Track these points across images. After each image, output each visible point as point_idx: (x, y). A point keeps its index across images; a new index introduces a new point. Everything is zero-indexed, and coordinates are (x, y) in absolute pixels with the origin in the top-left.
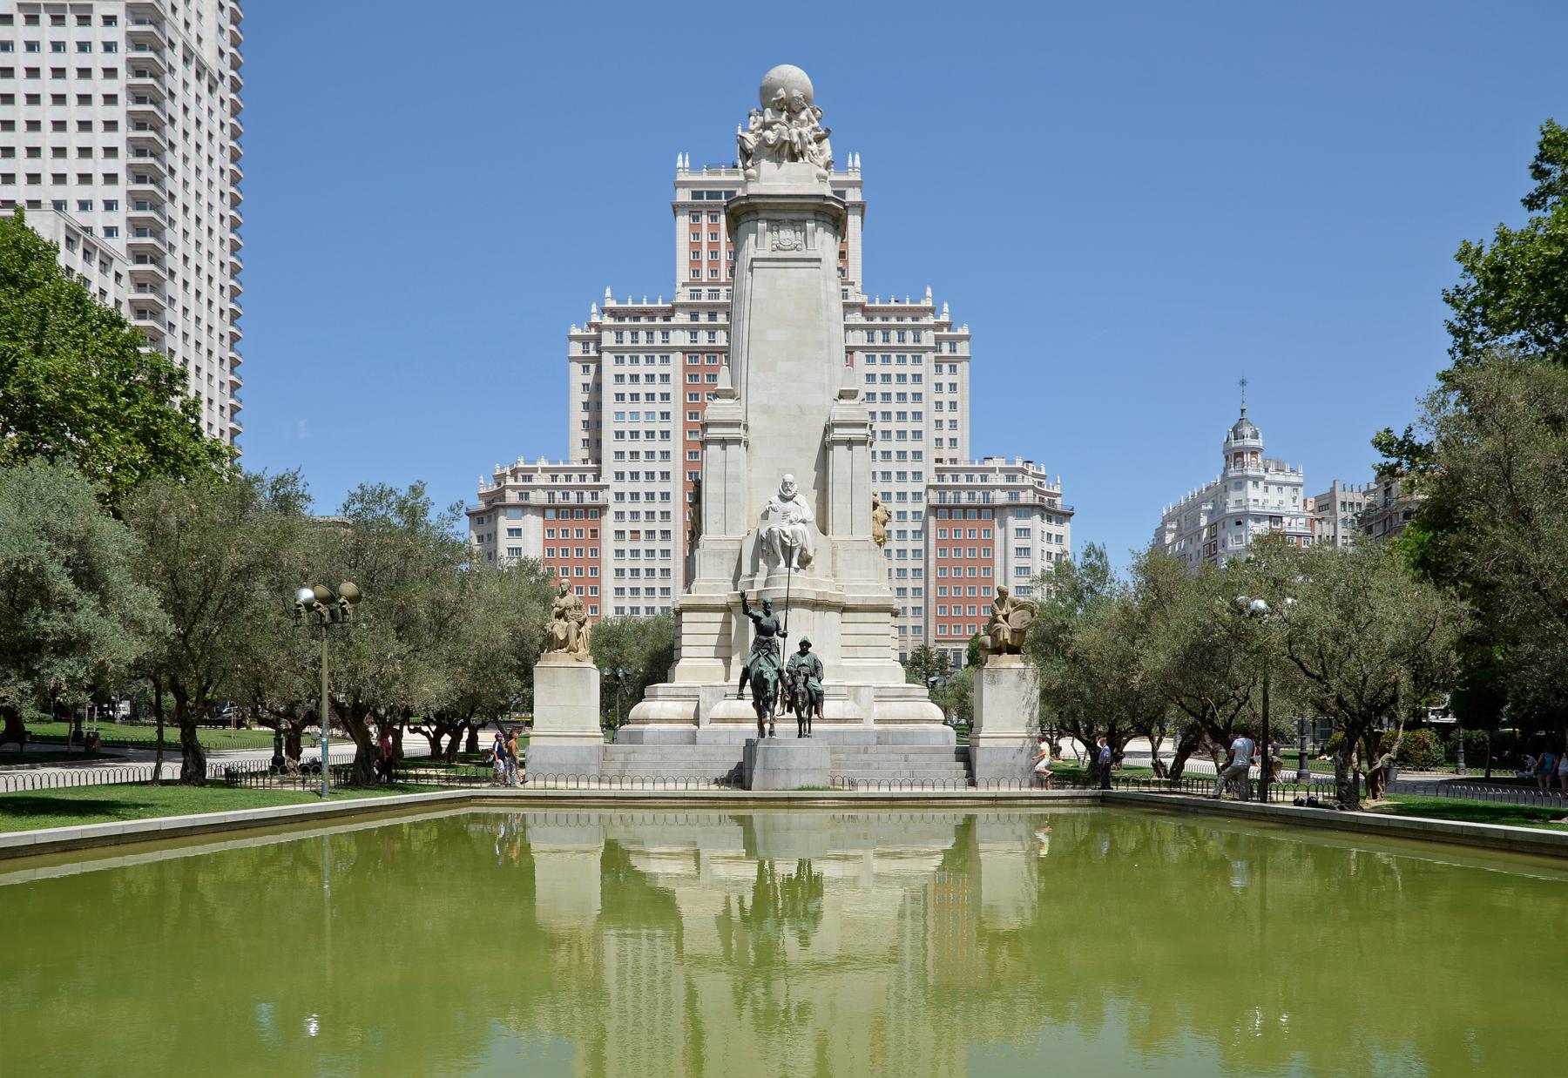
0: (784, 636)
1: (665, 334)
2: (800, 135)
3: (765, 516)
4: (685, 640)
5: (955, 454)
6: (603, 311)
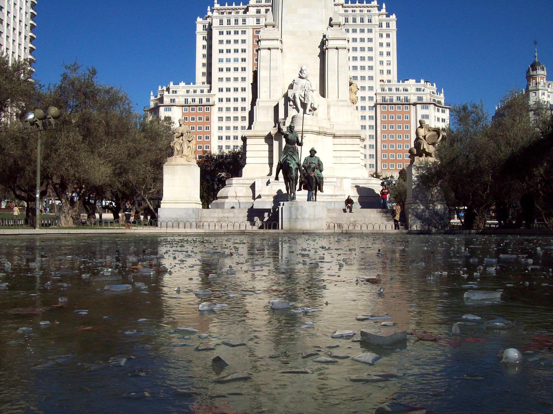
0: (301, 144)
1: (244, 21)
3: (291, 87)
4: (248, 154)
5: (390, 77)
6: (212, 11)
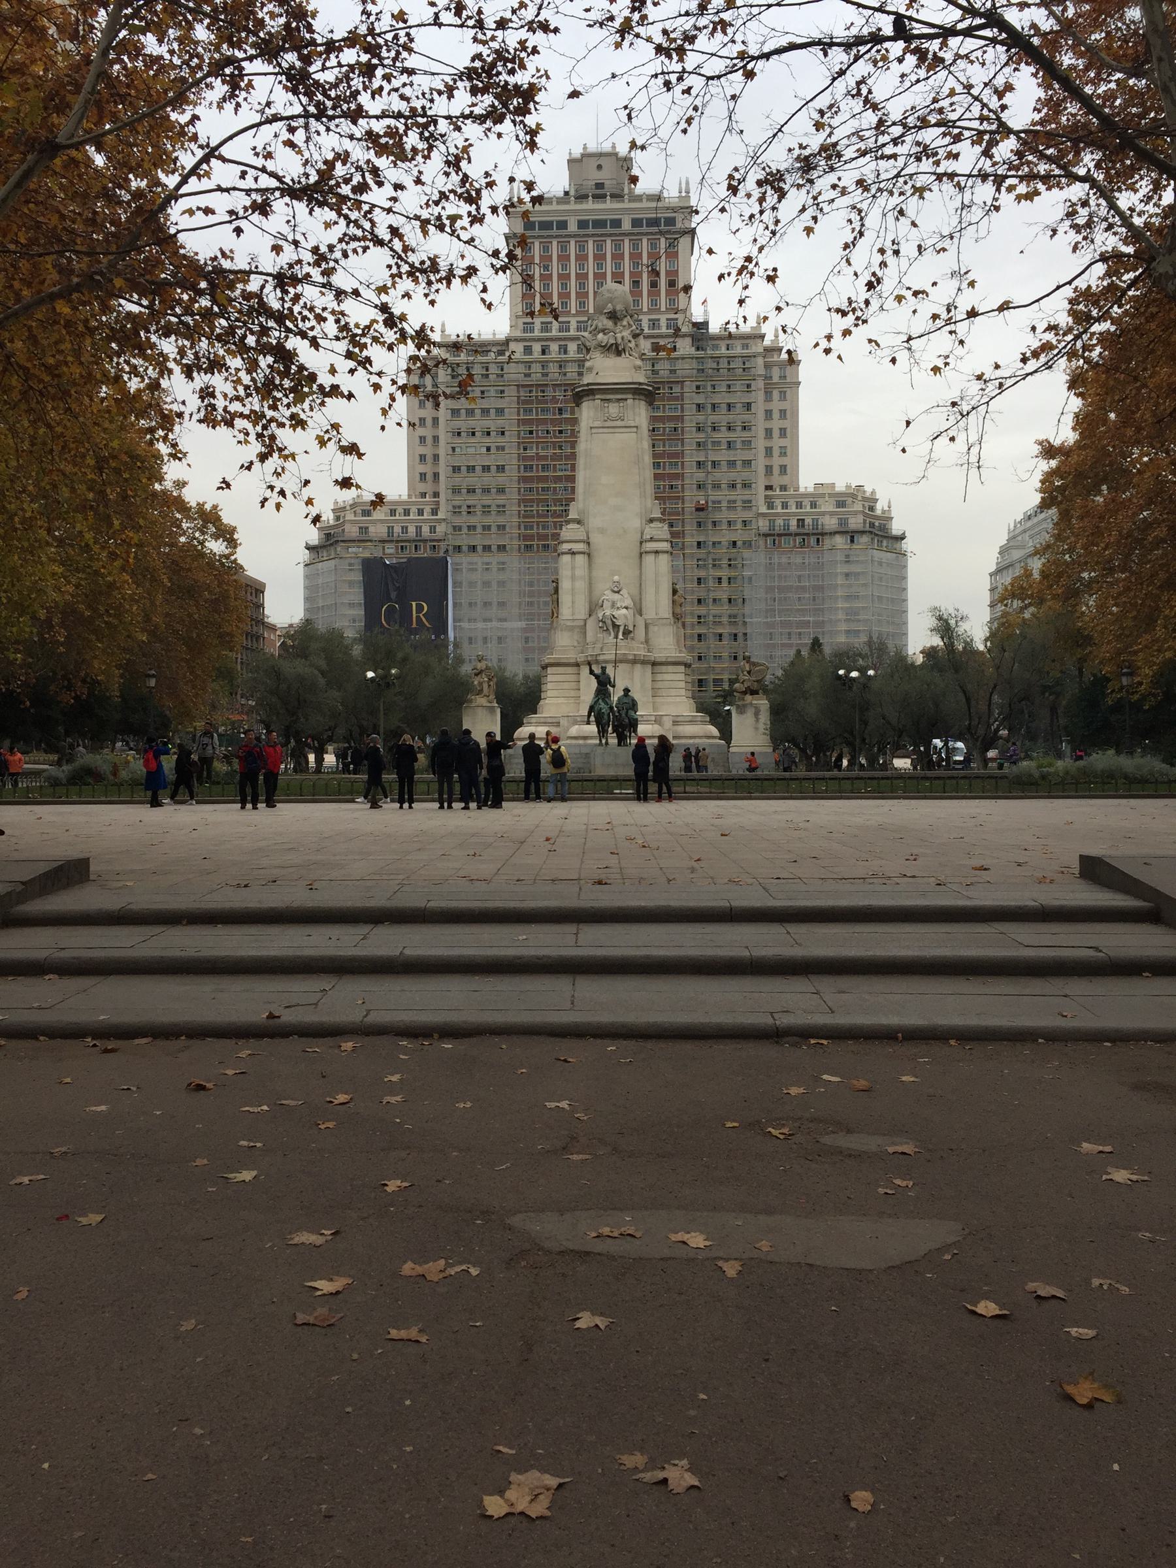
0: (614, 686)
2: (623, 338)
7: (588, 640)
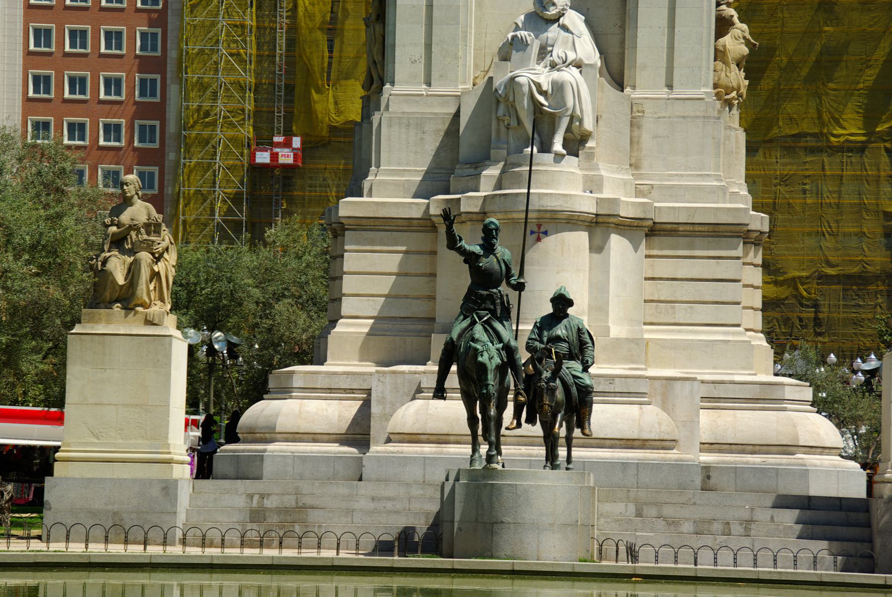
0: (520, 287)
4: (349, 284)
7: (464, 151)
